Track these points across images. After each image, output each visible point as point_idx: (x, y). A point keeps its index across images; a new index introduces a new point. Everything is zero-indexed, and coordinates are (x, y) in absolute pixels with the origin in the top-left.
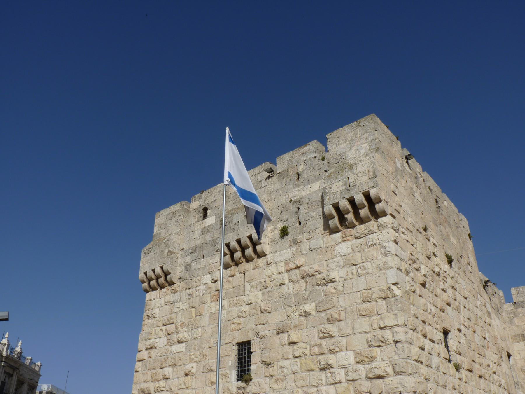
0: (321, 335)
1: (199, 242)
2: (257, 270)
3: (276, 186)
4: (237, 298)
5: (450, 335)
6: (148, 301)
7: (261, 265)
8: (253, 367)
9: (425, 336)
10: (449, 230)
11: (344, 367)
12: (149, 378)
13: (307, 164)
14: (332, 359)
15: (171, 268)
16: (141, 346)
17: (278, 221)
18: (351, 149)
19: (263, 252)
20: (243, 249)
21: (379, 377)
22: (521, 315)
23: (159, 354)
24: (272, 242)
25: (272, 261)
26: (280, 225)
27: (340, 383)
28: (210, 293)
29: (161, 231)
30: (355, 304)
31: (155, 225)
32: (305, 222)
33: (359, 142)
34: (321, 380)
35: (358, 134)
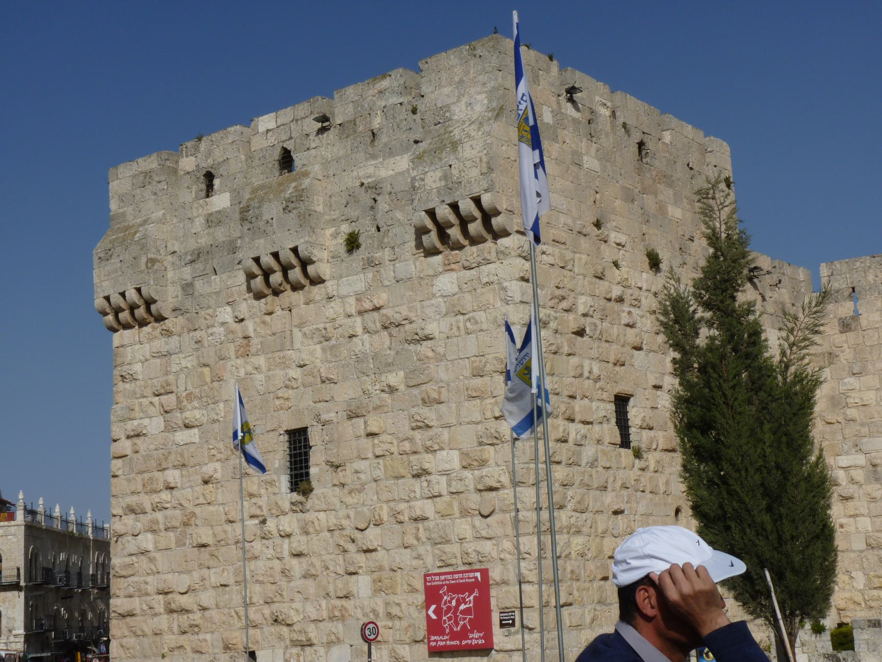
0: (414, 424)
1: (204, 241)
2: (312, 306)
3: (335, 150)
6: (117, 347)
7: (318, 298)
8: (313, 471)
10: (666, 193)
11: (446, 473)
12: (140, 488)
13: (388, 115)
14: (428, 461)
15: (157, 292)
16: (117, 431)
17: (343, 221)
18: (459, 100)
19: (320, 277)
20: (285, 269)
21: (491, 489)
22: (831, 316)
23: (152, 447)
24: (333, 257)
25: (335, 293)
26: (346, 229)
27: (440, 496)
28: (233, 341)
29: (126, 208)
30: (462, 377)
31: (110, 195)
32: (385, 228)
33: (471, 89)
34: (414, 492)
35: (472, 72)
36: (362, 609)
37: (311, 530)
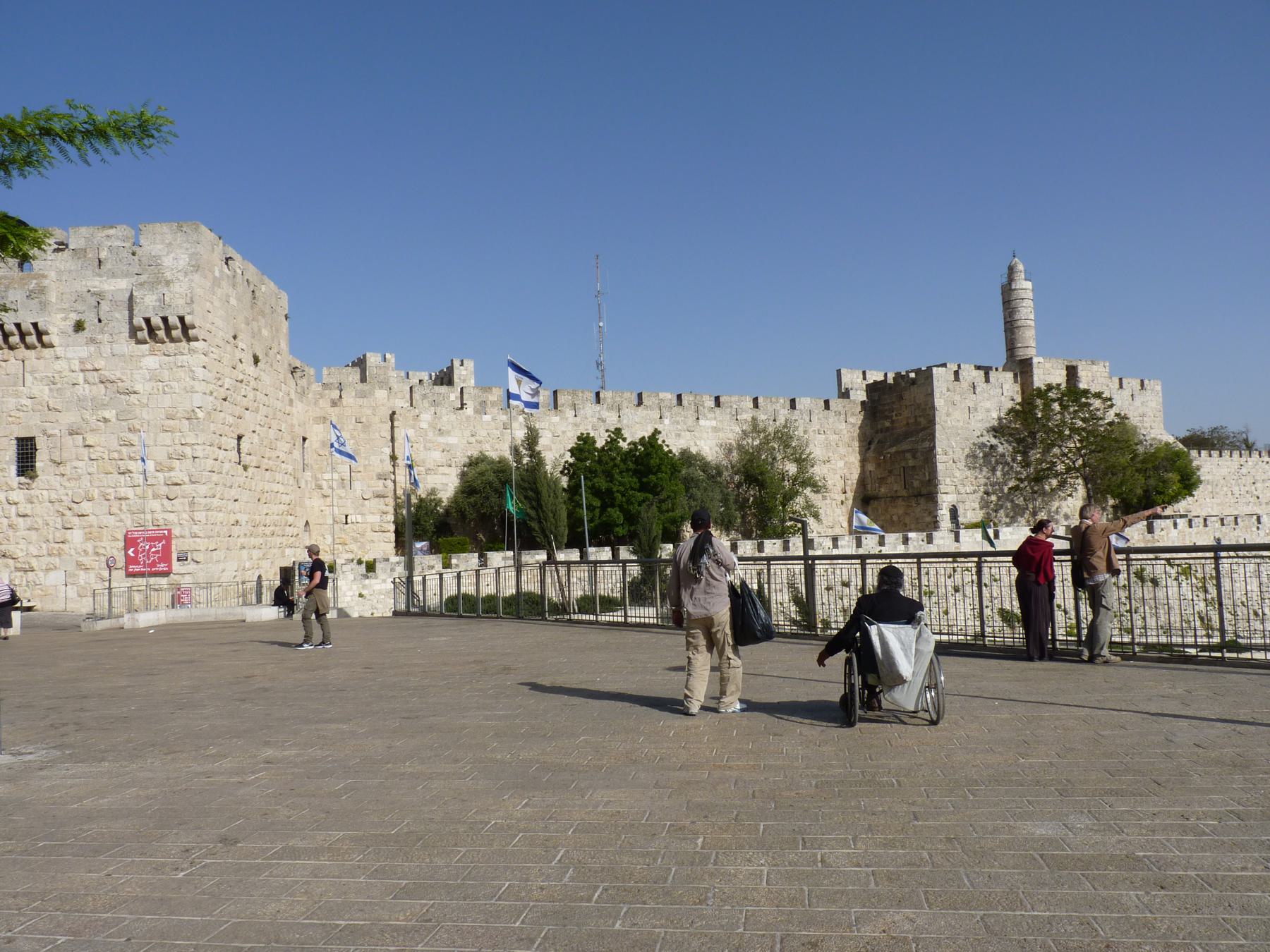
0: (122, 443)
2: (42, 361)
4: (14, 389)
5: (243, 439)
8: (38, 464)
9: (220, 448)
18: (167, 254)
19: (52, 343)
21: (176, 484)
26: (74, 317)
32: (106, 321)
36: (75, 550)
37: (35, 501)
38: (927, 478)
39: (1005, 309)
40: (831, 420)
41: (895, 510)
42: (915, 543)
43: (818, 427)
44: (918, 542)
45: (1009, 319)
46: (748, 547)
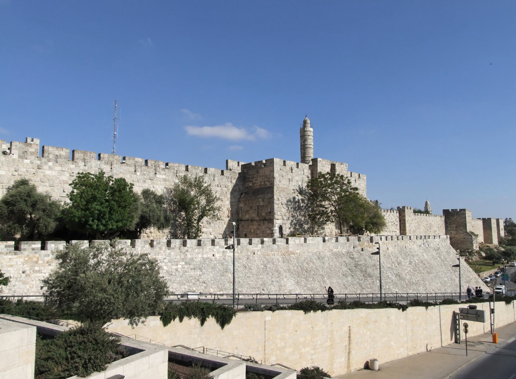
38: (269, 211)
39: (301, 139)
40: (224, 180)
41: (252, 227)
42: (267, 244)
43: (218, 183)
44: (268, 243)
45: (303, 144)
46: (177, 243)
